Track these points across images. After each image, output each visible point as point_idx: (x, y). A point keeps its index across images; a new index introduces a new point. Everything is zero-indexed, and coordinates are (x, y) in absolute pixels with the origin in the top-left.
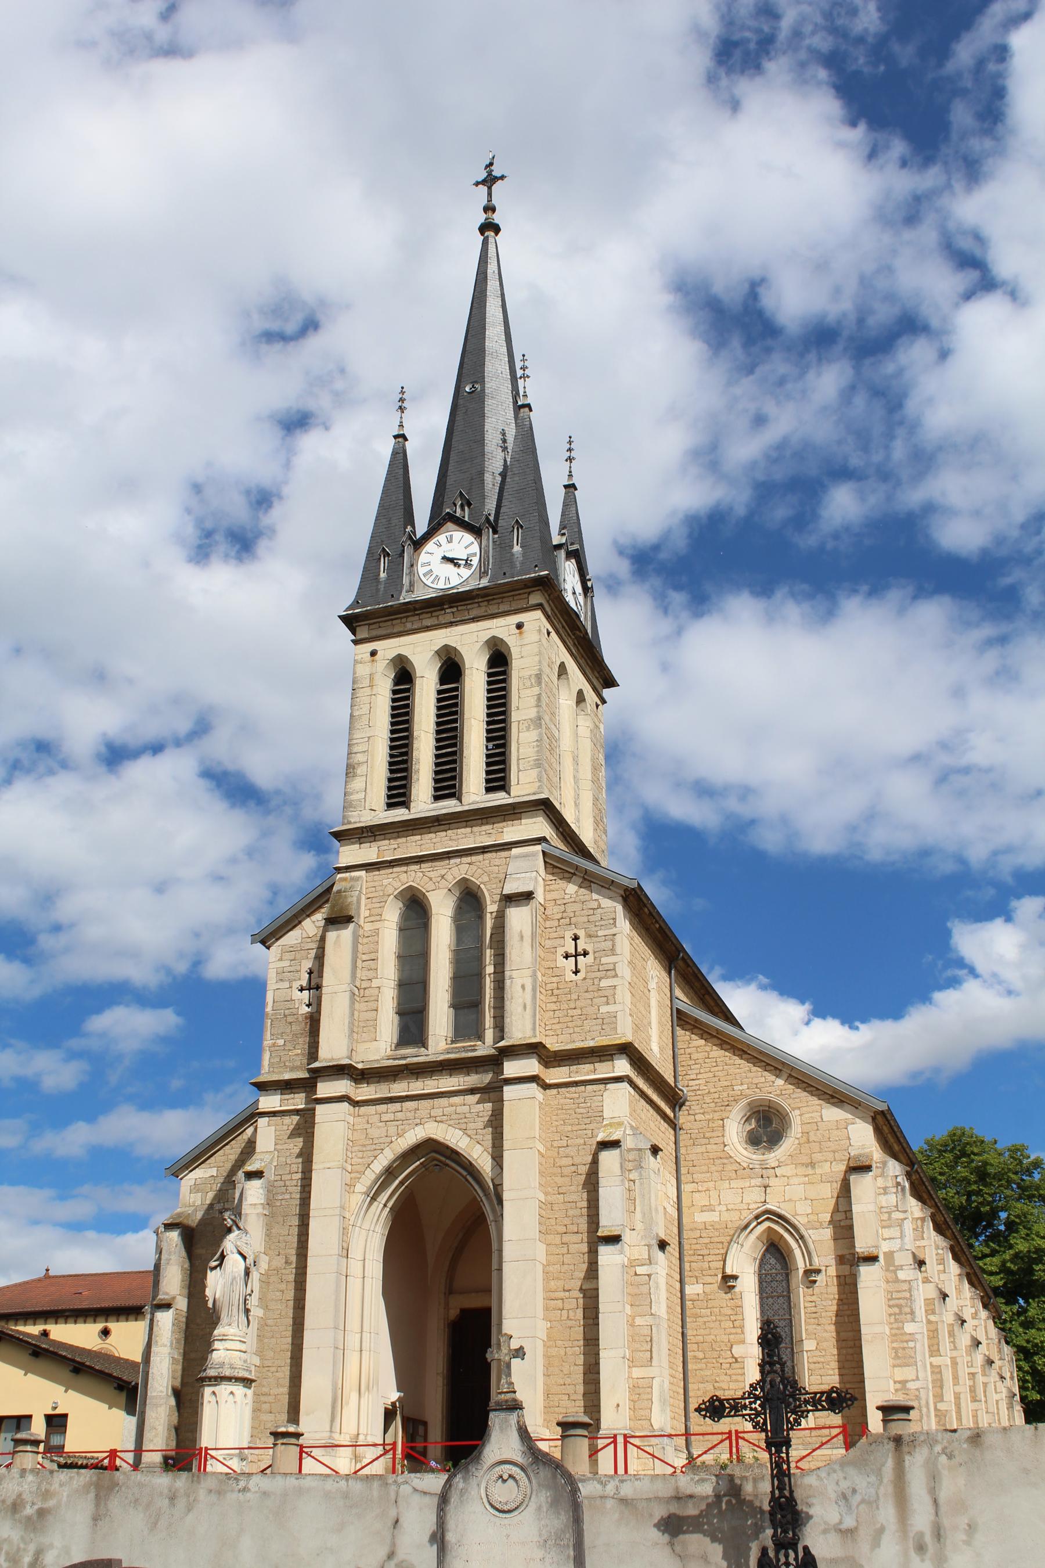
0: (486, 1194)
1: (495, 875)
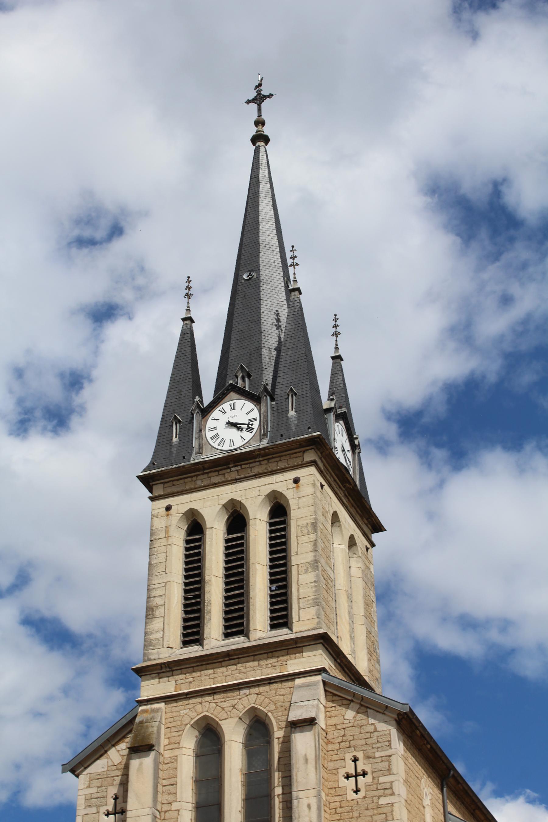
1: (281, 704)
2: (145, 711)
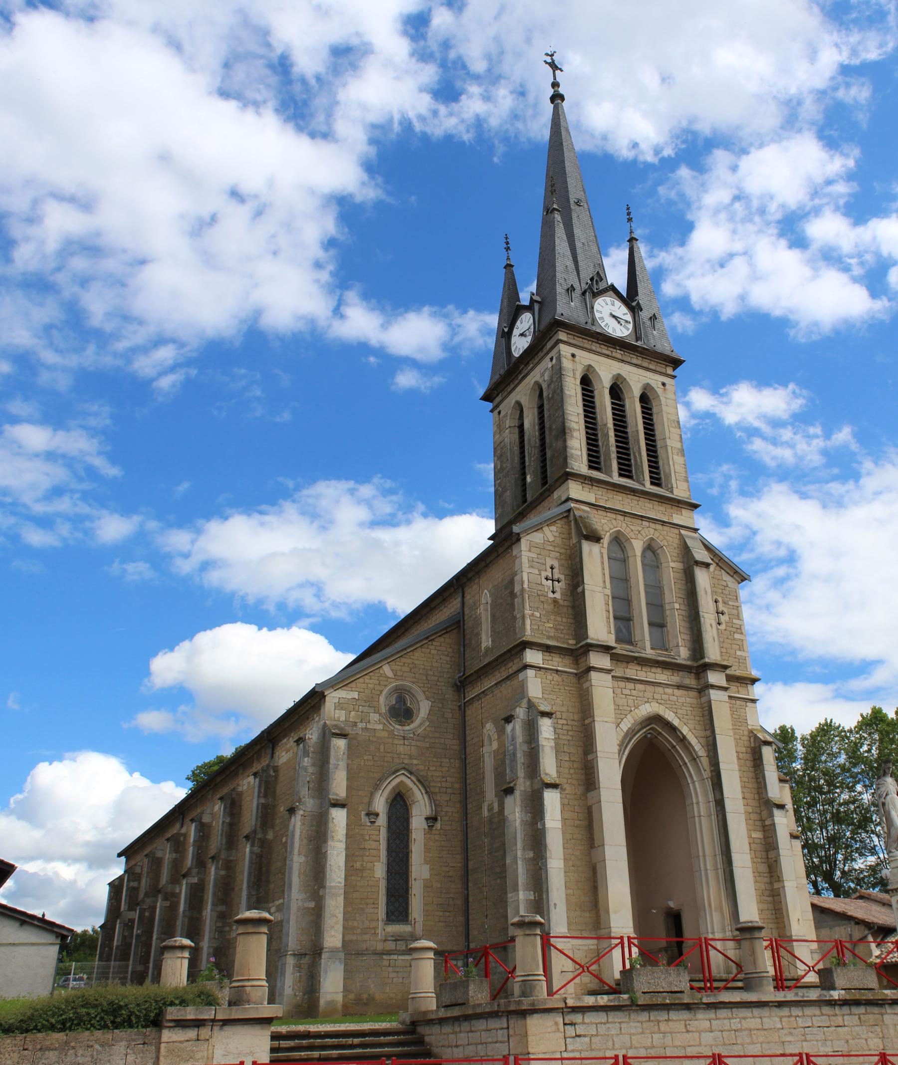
0: (694, 759)
2: (579, 509)
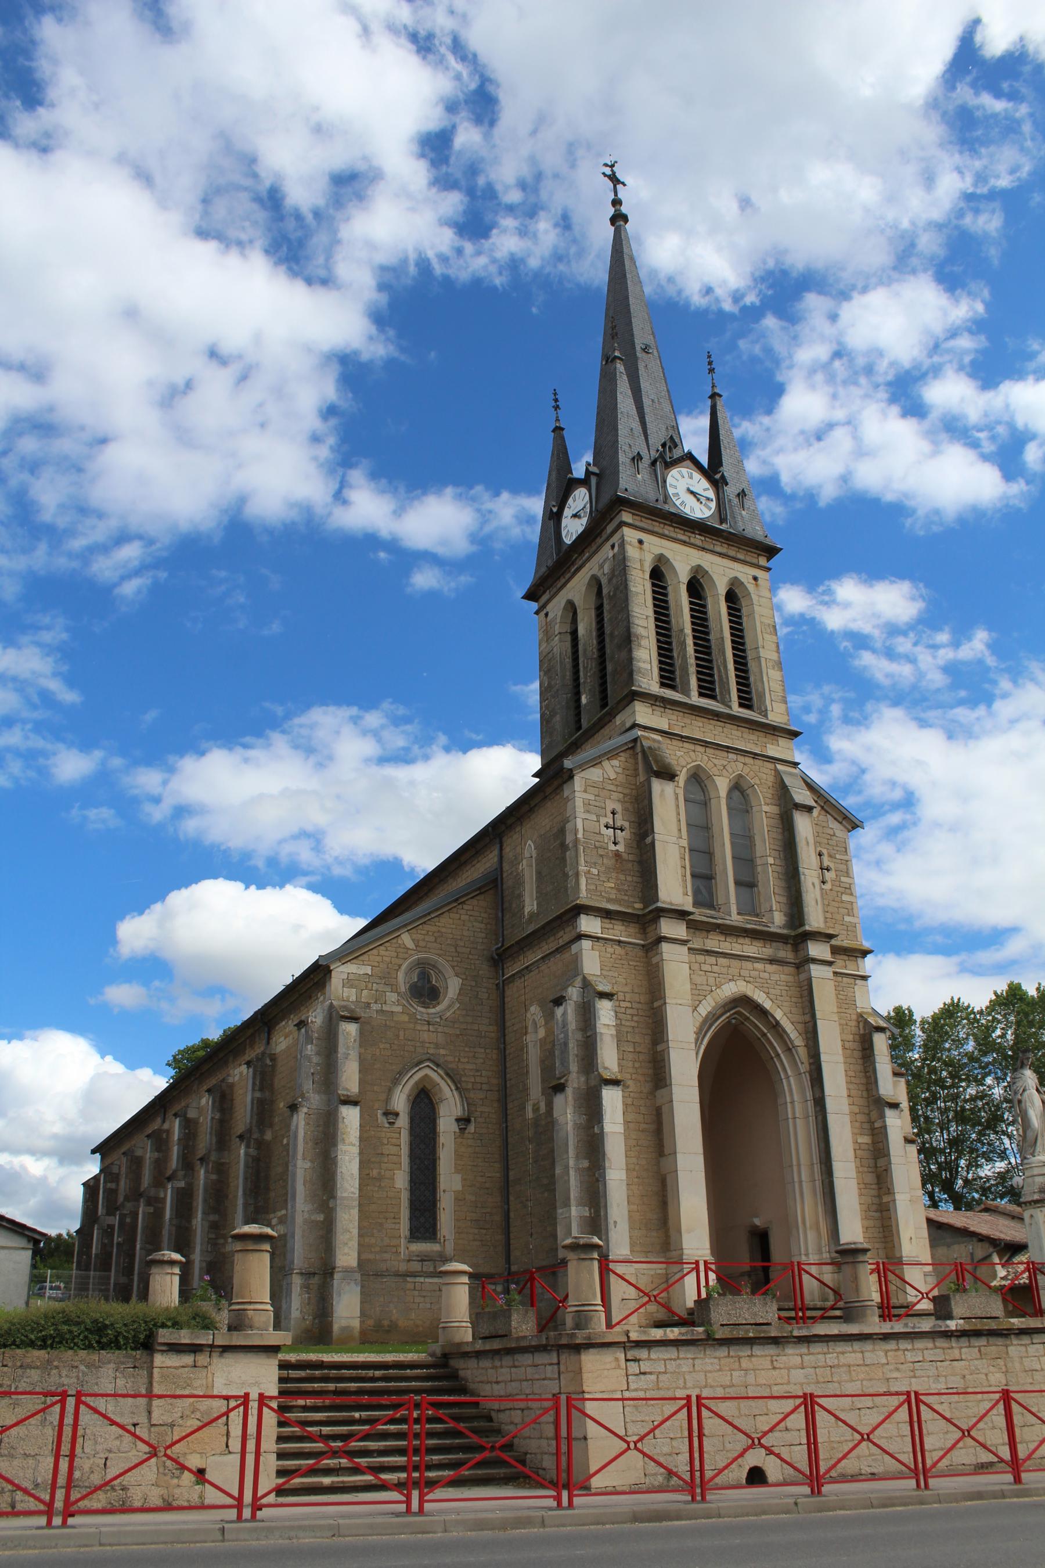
0: (789, 1050)
2: (648, 738)
